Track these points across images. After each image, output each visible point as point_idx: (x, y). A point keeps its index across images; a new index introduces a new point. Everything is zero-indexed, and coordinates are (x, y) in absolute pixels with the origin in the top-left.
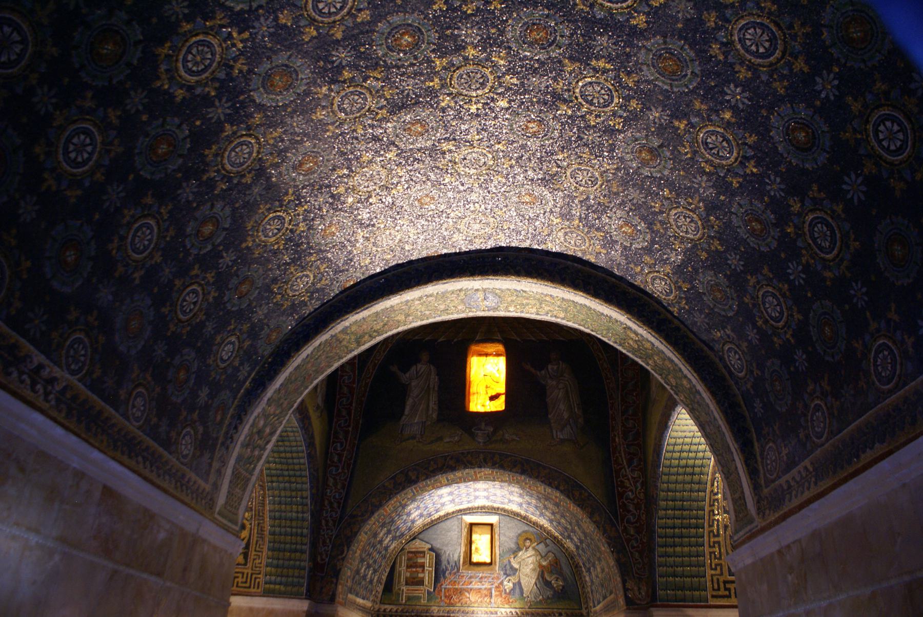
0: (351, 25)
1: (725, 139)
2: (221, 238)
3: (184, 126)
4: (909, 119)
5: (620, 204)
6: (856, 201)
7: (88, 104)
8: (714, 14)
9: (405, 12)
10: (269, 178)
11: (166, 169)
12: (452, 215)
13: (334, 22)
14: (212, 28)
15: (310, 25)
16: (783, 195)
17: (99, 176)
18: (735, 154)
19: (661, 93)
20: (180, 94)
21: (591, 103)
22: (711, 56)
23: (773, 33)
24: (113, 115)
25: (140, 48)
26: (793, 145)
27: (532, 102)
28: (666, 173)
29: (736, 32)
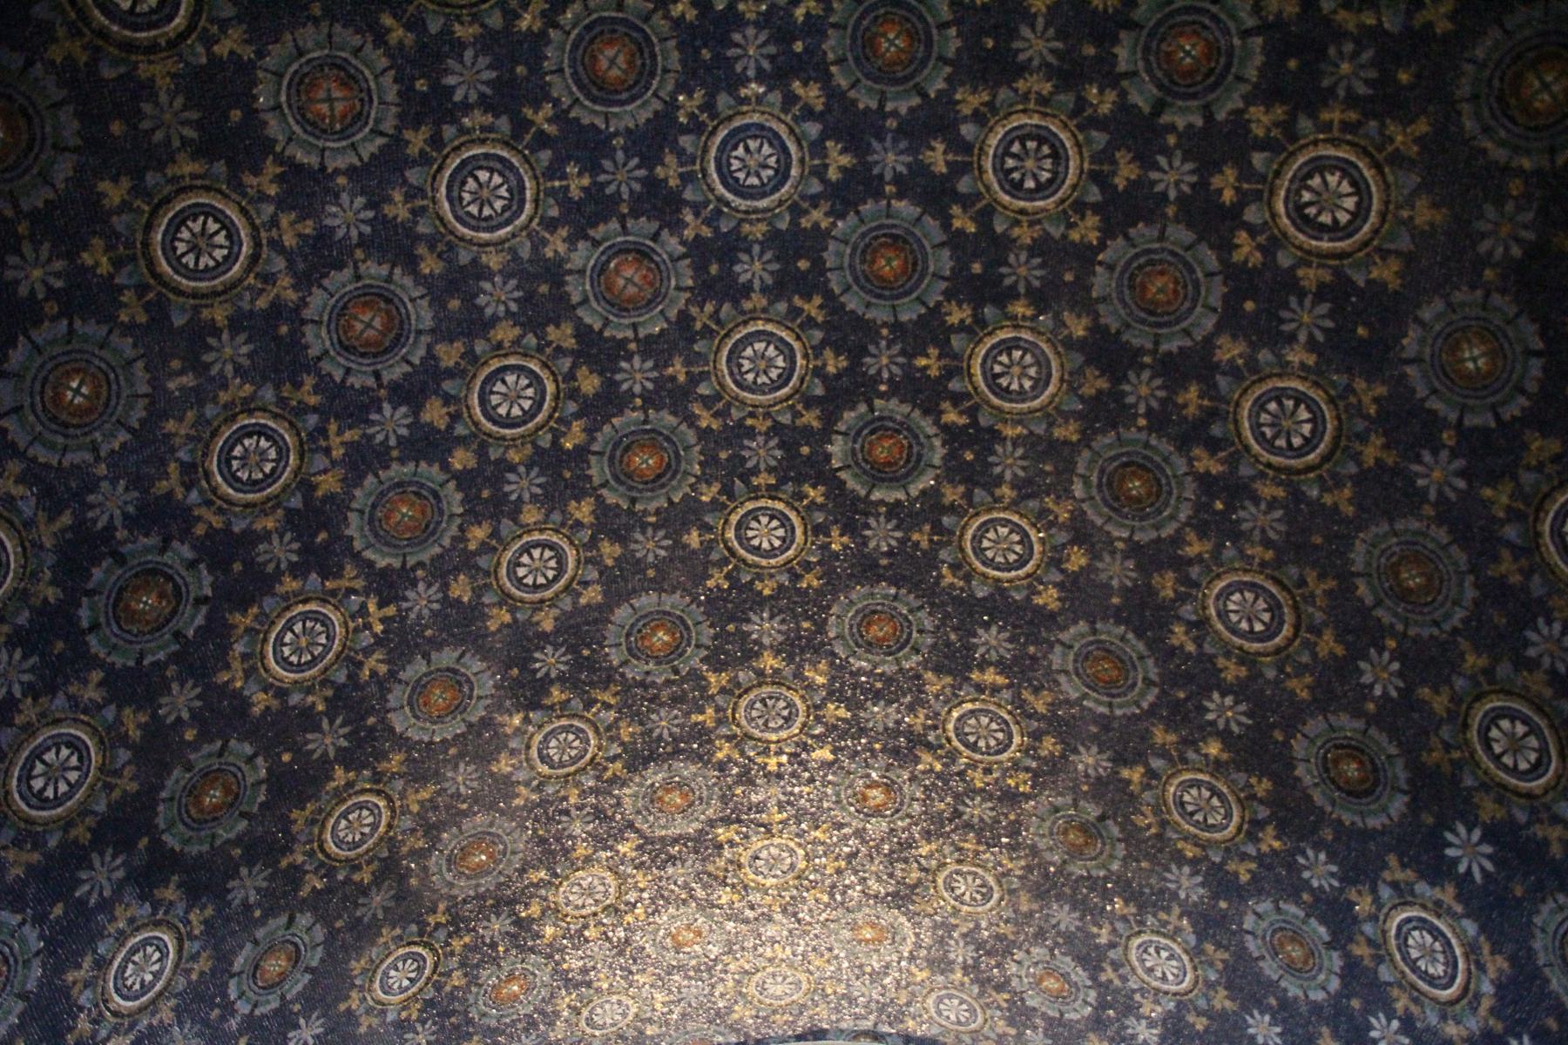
0: (568, 608)
1: (1215, 792)
2: (299, 987)
3: (260, 761)
4: (1539, 709)
5: (1036, 936)
6: (1478, 876)
7: (92, 694)
8: (1170, 575)
9: (660, 590)
10: (403, 878)
11: (214, 836)
12: (732, 967)
13: (542, 601)
14: (333, 593)
15: (500, 605)
16: (1336, 884)
17: (81, 833)
18: (1236, 819)
19: (1095, 723)
20: (260, 701)
21: (973, 747)
22: (1173, 648)
23: (1272, 596)
24: (133, 722)
25: (204, 609)
26: (1339, 788)
27: (872, 751)
28: (1115, 867)
29: (1211, 602)
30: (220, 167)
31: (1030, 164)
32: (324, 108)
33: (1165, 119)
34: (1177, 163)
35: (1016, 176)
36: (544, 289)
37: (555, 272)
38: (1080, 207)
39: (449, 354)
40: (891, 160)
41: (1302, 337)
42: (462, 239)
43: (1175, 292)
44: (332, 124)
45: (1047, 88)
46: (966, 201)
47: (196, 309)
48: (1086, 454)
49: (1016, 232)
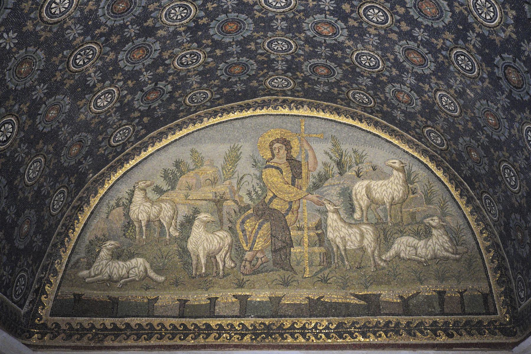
14: (466, 9)
30: (435, 108)
31: (189, 59)
32: (405, 97)
33: (154, 84)
34: (146, 79)
35: (193, 56)
36: (356, 35)
37: (350, 37)
38: (170, 57)
39: (394, 36)
40: (234, 49)
41: (93, 74)
42: (379, 56)
43: (133, 56)
44: (404, 94)
45: (189, 73)
46: (208, 46)
47: (457, 98)
48: (143, 5)
49: (189, 45)
